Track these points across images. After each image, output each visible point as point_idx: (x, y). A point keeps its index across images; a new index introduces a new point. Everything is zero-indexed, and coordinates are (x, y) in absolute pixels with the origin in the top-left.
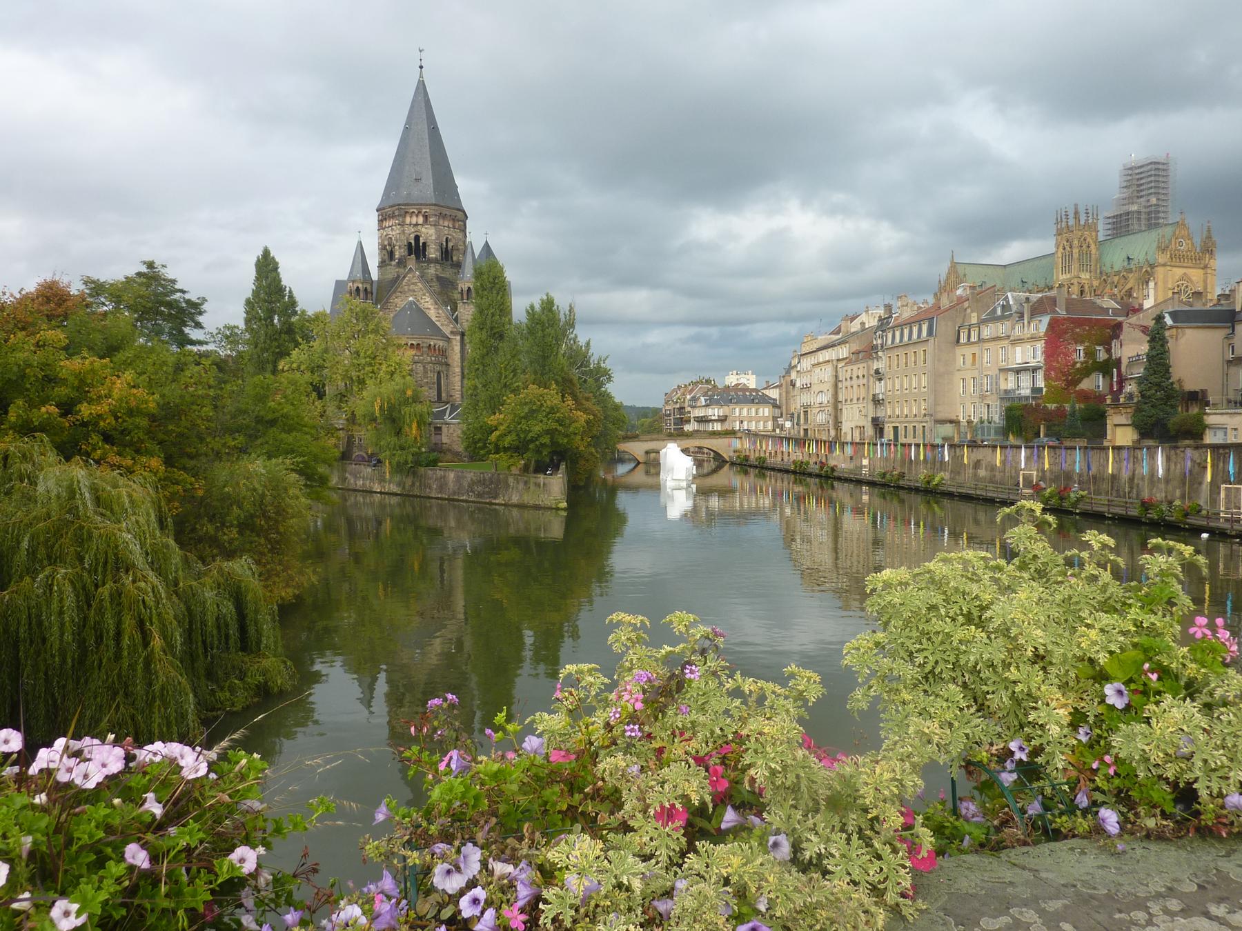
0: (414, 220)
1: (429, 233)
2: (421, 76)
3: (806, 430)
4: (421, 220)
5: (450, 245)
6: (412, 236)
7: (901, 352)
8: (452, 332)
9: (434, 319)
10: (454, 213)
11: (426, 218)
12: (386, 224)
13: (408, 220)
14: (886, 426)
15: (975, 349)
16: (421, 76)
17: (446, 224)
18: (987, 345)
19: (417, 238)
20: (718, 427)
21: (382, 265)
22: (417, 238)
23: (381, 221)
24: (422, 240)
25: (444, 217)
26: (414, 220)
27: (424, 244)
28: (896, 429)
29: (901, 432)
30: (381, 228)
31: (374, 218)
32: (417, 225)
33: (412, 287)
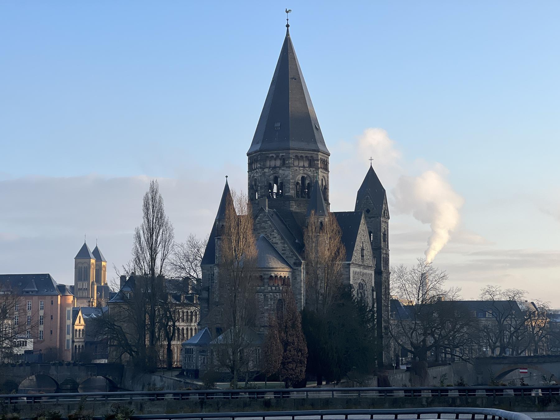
0: (273, 163)
2: (288, 34)
4: (278, 163)
5: (307, 182)
6: (272, 177)
8: (295, 264)
9: (281, 252)
10: (309, 154)
11: (283, 160)
13: (268, 164)
16: (288, 34)
17: (301, 164)
23: (250, 164)
24: (279, 180)
25: (297, 158)
26: (273, 163)
27: (282, 183)
30: (251, 170)
31: (245, 160)
32: (275, 167)
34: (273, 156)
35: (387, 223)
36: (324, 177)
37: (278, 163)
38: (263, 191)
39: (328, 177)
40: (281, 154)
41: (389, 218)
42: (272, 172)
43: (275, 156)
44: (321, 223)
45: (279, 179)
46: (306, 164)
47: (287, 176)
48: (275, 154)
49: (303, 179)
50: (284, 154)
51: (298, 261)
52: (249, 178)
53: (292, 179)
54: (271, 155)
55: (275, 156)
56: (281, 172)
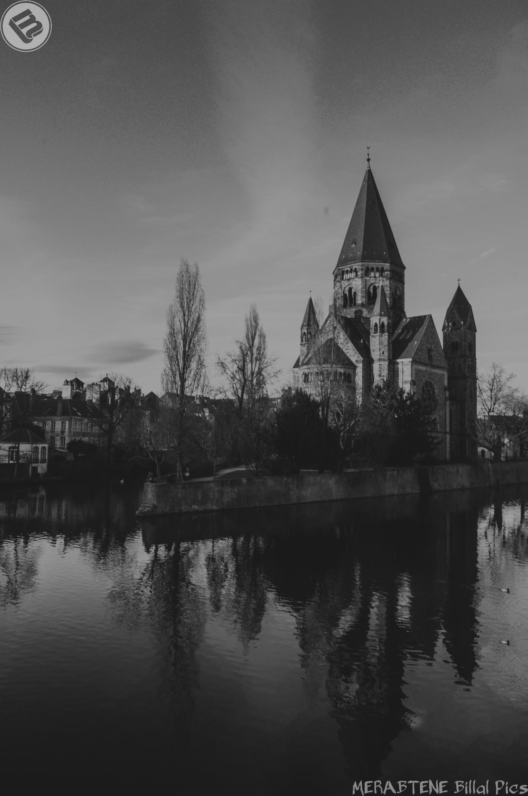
1: (357, 284)
6: (347, 289)
8: (356, 361)
19: (350, 289)
22: (350, 289)
24: (353, 291)
27: (355, 293)
34: (347, 271)
35: (475, 335)
36: (396, 286)
37: (353, 275)
38: (340, 301)
39: (403, 288)
40: (354, 267)
41: (476, 331)
42: (347, 284)
43: (349, 269)
44: (383, 323)
45: (353, 290)
46: (377, 275)
47: (358, 287)
48: (350, 267)
50: (357, 267)
51: (359, 359)
53: (362, 288)
54: (346, 269)
55: (349, 269)
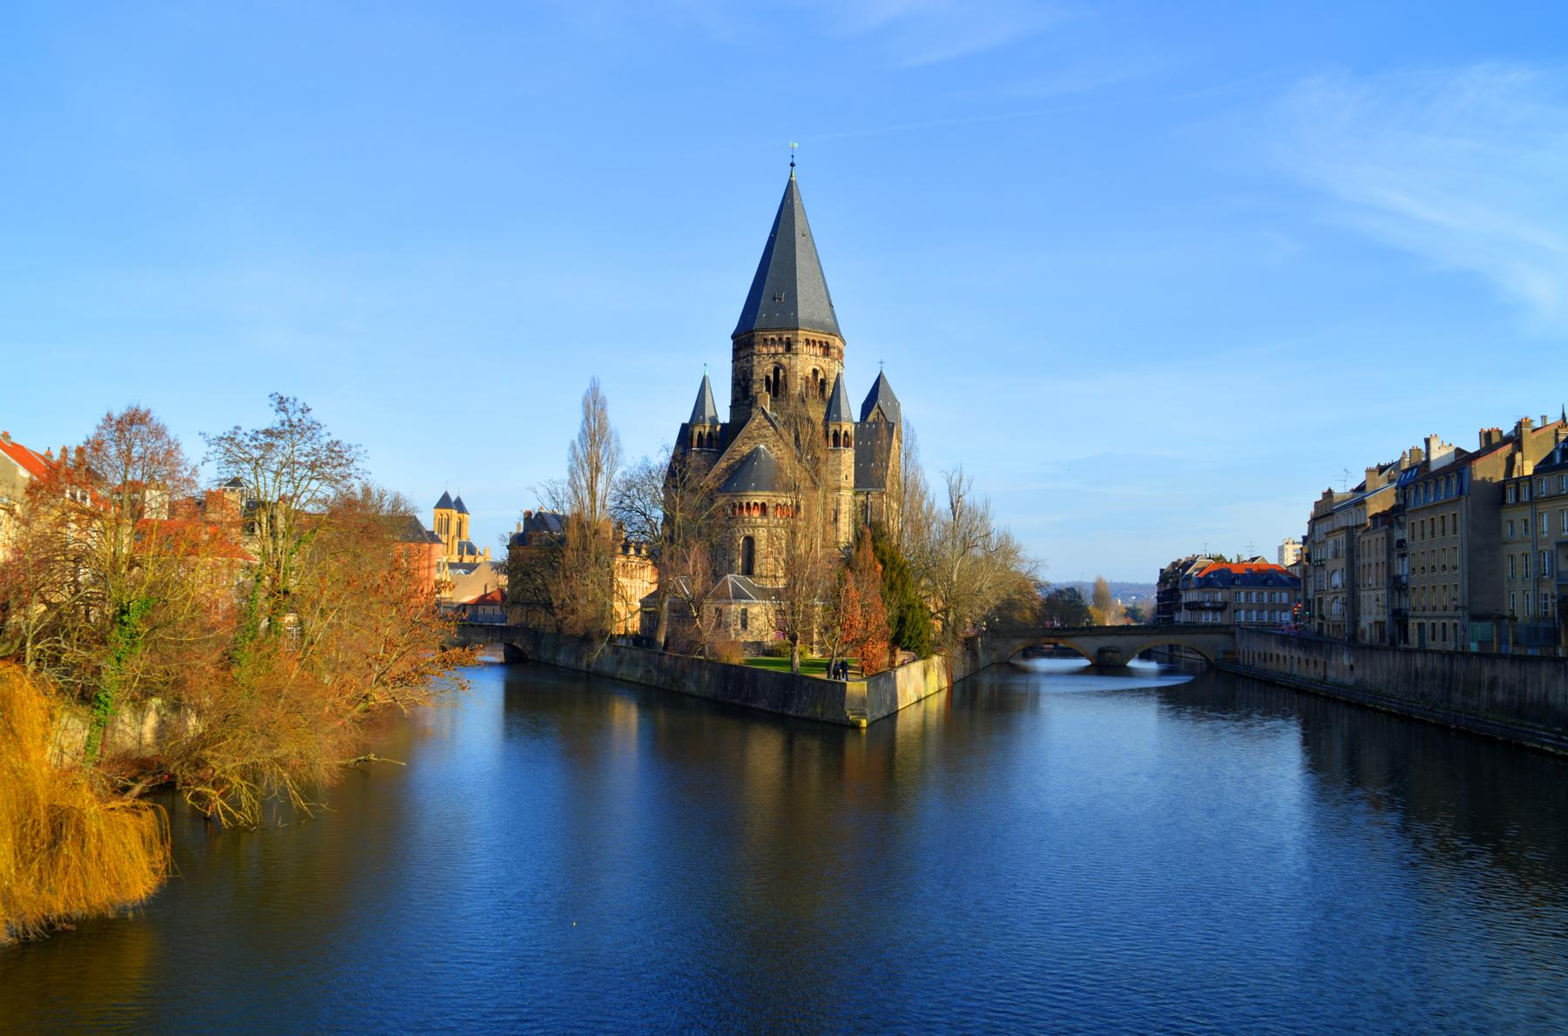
3: (1320, 625)
4: (780, 350)
5: (820, 376)
6: (771, 367)
7: (1426, 517)
10: (824, 338)
12: (742, 354)
14: (1411, 621)
15: (1526, 513)
18: (1541, 507)
20: (1208, 618)
21: (734, 406)
23: (736, 351)
28: (1421, 625)
29: (1428, 632)
32: (776, 354)
33: (764, 431)
37: (780, 350)
49: (815, 372)
52: (734, 370)
56: (784, 361)
